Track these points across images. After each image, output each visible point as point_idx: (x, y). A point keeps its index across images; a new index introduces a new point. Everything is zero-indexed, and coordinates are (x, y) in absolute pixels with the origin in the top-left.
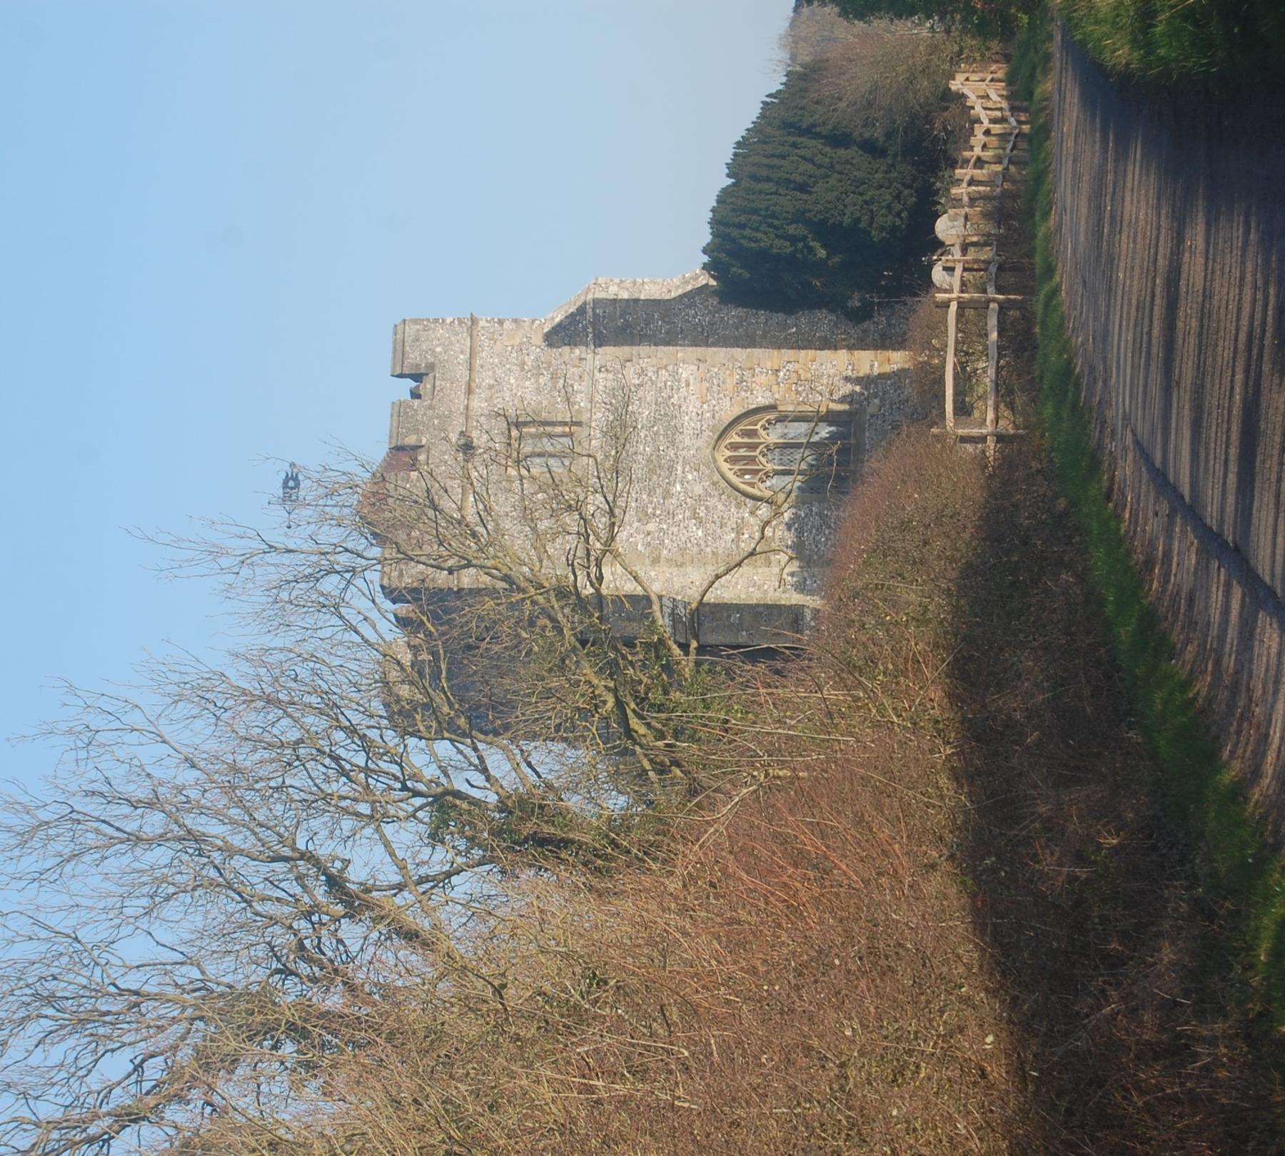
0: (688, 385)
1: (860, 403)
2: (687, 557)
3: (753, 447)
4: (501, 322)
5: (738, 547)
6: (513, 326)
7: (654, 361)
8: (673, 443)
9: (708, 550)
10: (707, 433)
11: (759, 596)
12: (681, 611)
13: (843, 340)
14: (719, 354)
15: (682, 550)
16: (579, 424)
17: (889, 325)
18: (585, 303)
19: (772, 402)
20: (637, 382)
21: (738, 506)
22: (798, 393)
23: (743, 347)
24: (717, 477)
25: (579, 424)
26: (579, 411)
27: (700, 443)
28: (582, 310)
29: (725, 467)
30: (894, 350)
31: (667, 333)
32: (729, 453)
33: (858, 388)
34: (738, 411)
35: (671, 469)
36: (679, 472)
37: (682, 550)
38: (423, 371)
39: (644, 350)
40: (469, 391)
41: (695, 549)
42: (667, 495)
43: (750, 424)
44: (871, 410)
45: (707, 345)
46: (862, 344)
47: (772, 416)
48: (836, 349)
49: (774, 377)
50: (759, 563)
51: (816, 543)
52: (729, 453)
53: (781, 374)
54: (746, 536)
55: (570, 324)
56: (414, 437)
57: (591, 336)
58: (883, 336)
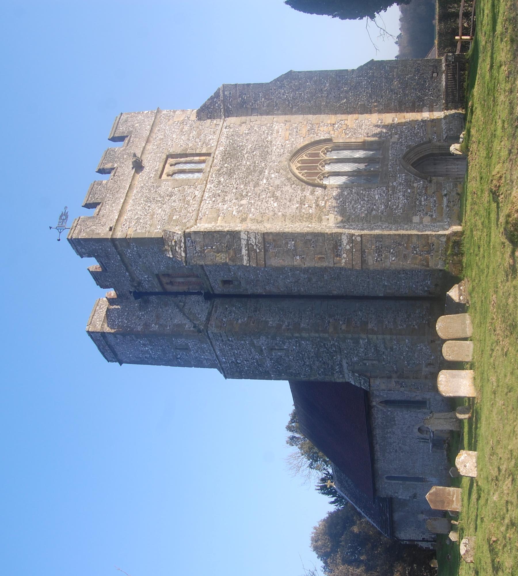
1: (386, 137)
3: (317, 161)
4: (174, 112)
5: (300, 212)
6: (181, 113)
7: (259, 122)
8: (265, 159)
9: (280, 214)
10: (287, 154)
12: (253, 241)
13: (375, 106)
14: (298, 118)
15: (263, 214)
16: (209, 155)
17: (405, 95)
18: (219, 89)
19: (327, 136)
20: (247, 132)
21: (303, 190)
22: (346, 134)
23: (314, 114)
24: (290, 175)
25: (209, 155)
26: (210, 148)
27: (283, 159)
28: (217, 95)
29: (297, 172)
30: (407, 112)
31: (267, 106)
33: (384, 131)
34: (307, 143)
35: (261, 172)
36: (266, 173)
37: (263, 214)
38: (125, 135)
39: (253, 118)
40: (148, 141)
41: (271, 213)
42: (257, 185)
43: (314, 151)
44: (393, 140)
45: (292, 113)
46: (387, 109)
47: (329, 146)
48: (371, 113)
49: (331, 128)
50: (314, 220)
51: (354, 209)
52: (299, 165)
53: (337, 126)
54: (307, 206)
55: (211, 103)
56: (111, 164)
57: (222, 110)
58: (400, 103)
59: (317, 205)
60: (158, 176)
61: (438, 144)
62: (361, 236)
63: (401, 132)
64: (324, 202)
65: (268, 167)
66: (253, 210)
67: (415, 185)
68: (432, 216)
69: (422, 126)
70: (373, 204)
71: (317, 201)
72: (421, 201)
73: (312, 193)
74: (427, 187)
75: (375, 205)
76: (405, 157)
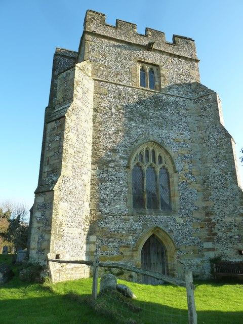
0: (181, 134)
2: (97, 125)
11: (70, 151)
21: (125, 151)
27: (155, 136)
32: (151, 149)
35: (142, 122)
36: (141, 126)
59: (110, 162)
60: (140, 60)
61: (176, 256)
62: (53, 191)
63: (186, 225)
64: (113, 166)
65: (147, 127)
66: (106, 116)
67: (130, 237)
68: (96, 252)
69: (194, 242)
70: (110, 203)
71: (114, 161)
72: (113, 242)
73: (121, 158)
74: (128, 247)
75: (109, 205)
76: (157, 229)
